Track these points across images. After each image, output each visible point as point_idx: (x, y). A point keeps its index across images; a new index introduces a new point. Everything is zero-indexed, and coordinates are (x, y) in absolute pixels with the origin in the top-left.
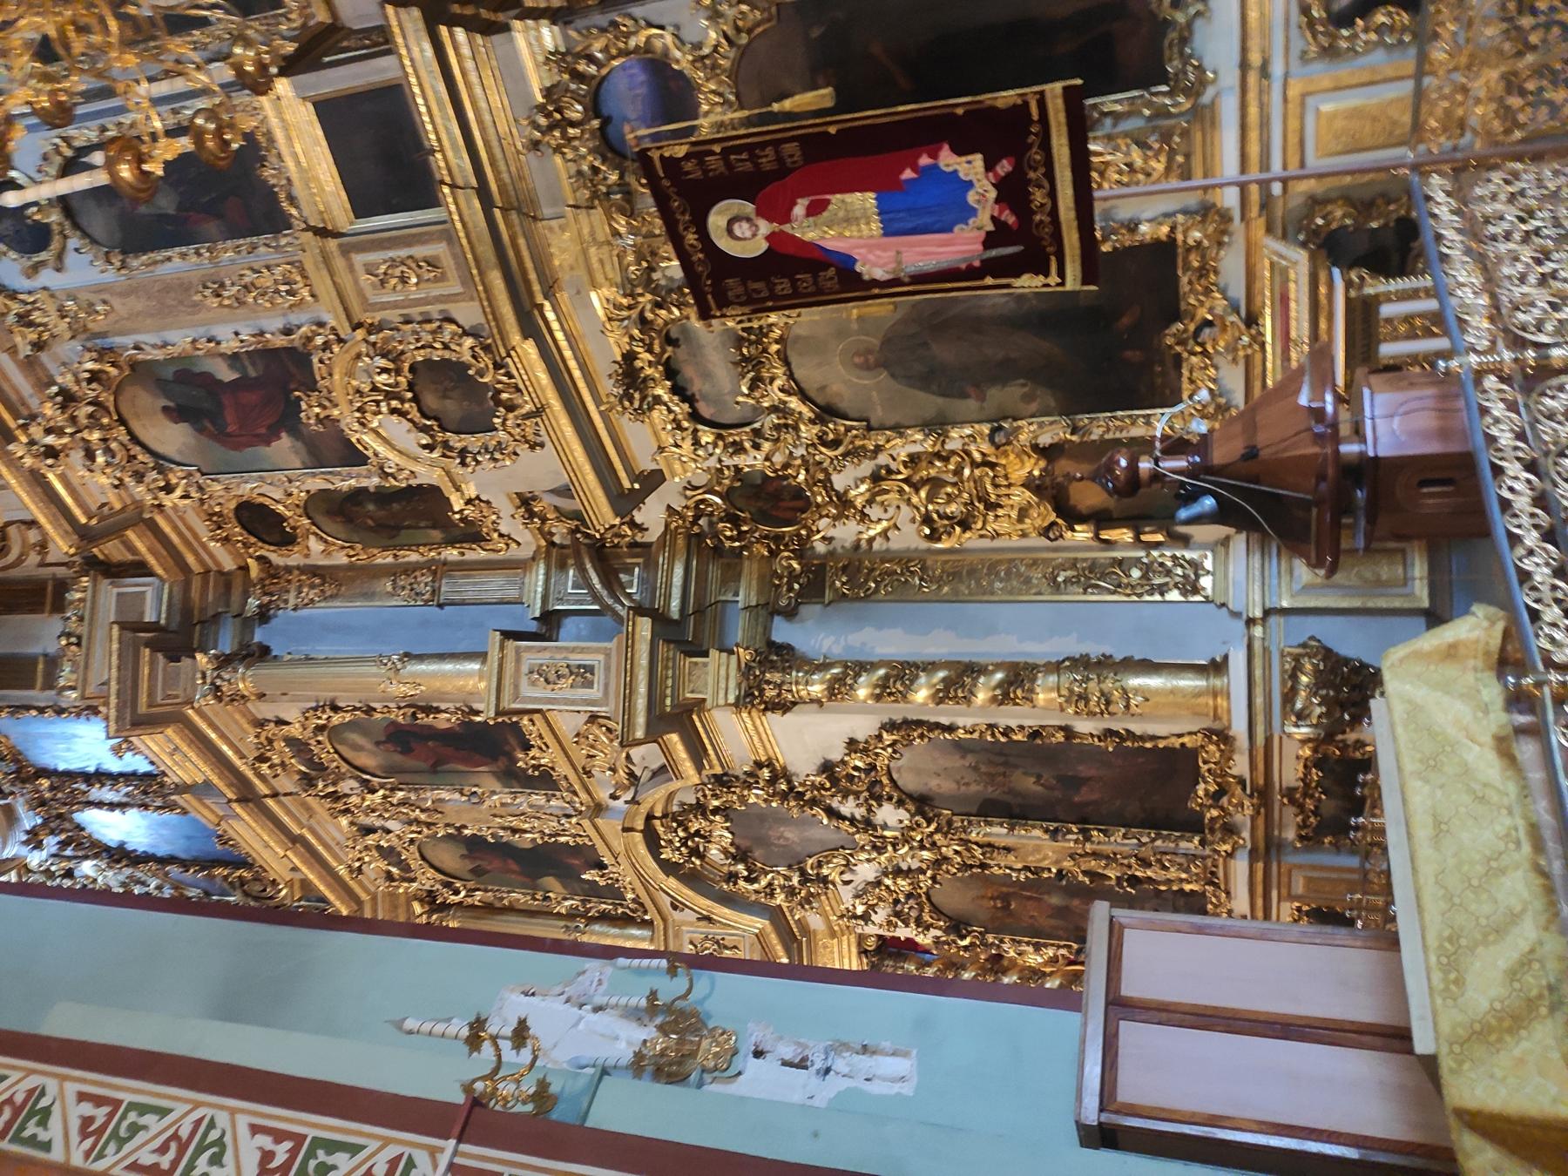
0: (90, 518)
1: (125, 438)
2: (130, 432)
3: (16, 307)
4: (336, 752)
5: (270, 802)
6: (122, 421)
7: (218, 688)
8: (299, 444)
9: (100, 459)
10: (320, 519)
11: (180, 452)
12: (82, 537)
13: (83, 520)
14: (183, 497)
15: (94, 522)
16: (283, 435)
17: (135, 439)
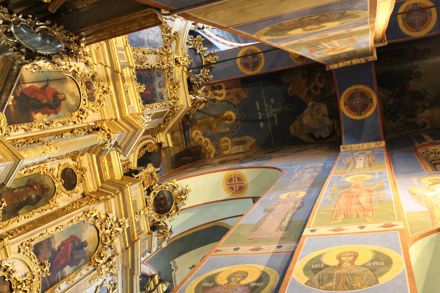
0: (118, 194)
1: (100, 231)
2: (98, 233)
3: (111, 271)
4: (80, 93)
5: (109, 64)
6: (99, 237)
7: (109, 138)
8: (53, 246)
9: (110, 224)
10: (51, 186)
11: (87, 228)
12: (123, 190)
13: (120, 194)
14: (92, 214)
15: (117, 192)
16: (57, 249)
17: (98, 231)
